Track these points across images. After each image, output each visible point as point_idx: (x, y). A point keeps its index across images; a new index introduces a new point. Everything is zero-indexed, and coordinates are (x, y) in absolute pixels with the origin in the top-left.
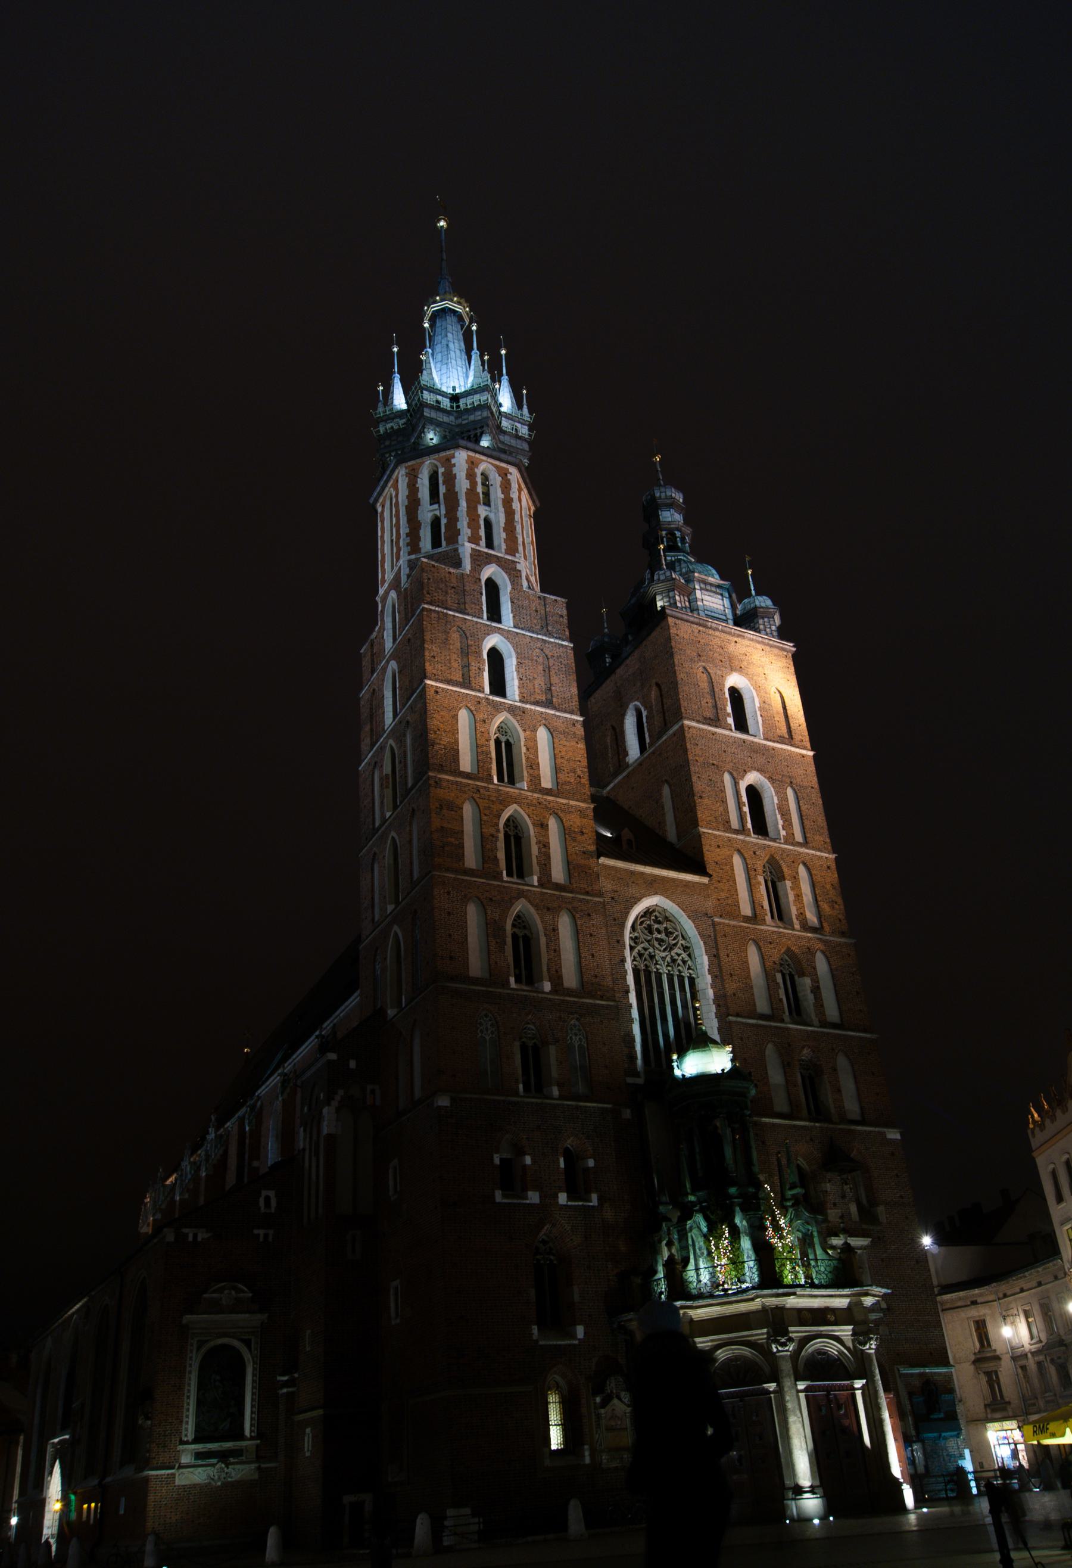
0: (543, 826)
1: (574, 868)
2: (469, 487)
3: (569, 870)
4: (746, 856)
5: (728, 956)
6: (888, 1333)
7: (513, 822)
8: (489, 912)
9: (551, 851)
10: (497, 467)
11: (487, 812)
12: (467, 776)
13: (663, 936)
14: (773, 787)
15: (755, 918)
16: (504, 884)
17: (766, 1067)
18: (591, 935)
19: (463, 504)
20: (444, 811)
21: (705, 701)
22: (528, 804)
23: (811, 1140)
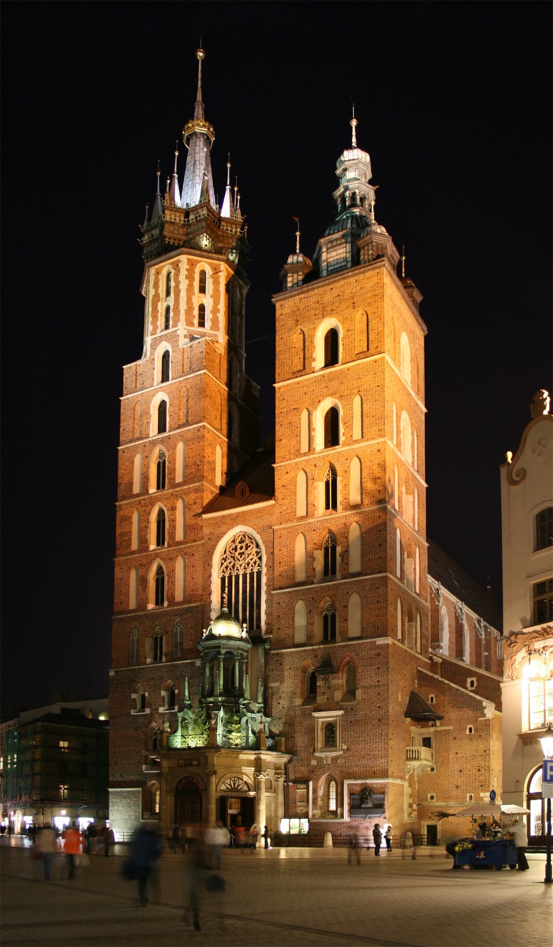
0: (173, 509)
2: (154, 294)
5: (280, 550)
6: (344, 763)
7: (163, 511)
10: (172, 264)
16: (149, 553)
17: (293, 617)
20: (123, 523)
23: (316, 657)
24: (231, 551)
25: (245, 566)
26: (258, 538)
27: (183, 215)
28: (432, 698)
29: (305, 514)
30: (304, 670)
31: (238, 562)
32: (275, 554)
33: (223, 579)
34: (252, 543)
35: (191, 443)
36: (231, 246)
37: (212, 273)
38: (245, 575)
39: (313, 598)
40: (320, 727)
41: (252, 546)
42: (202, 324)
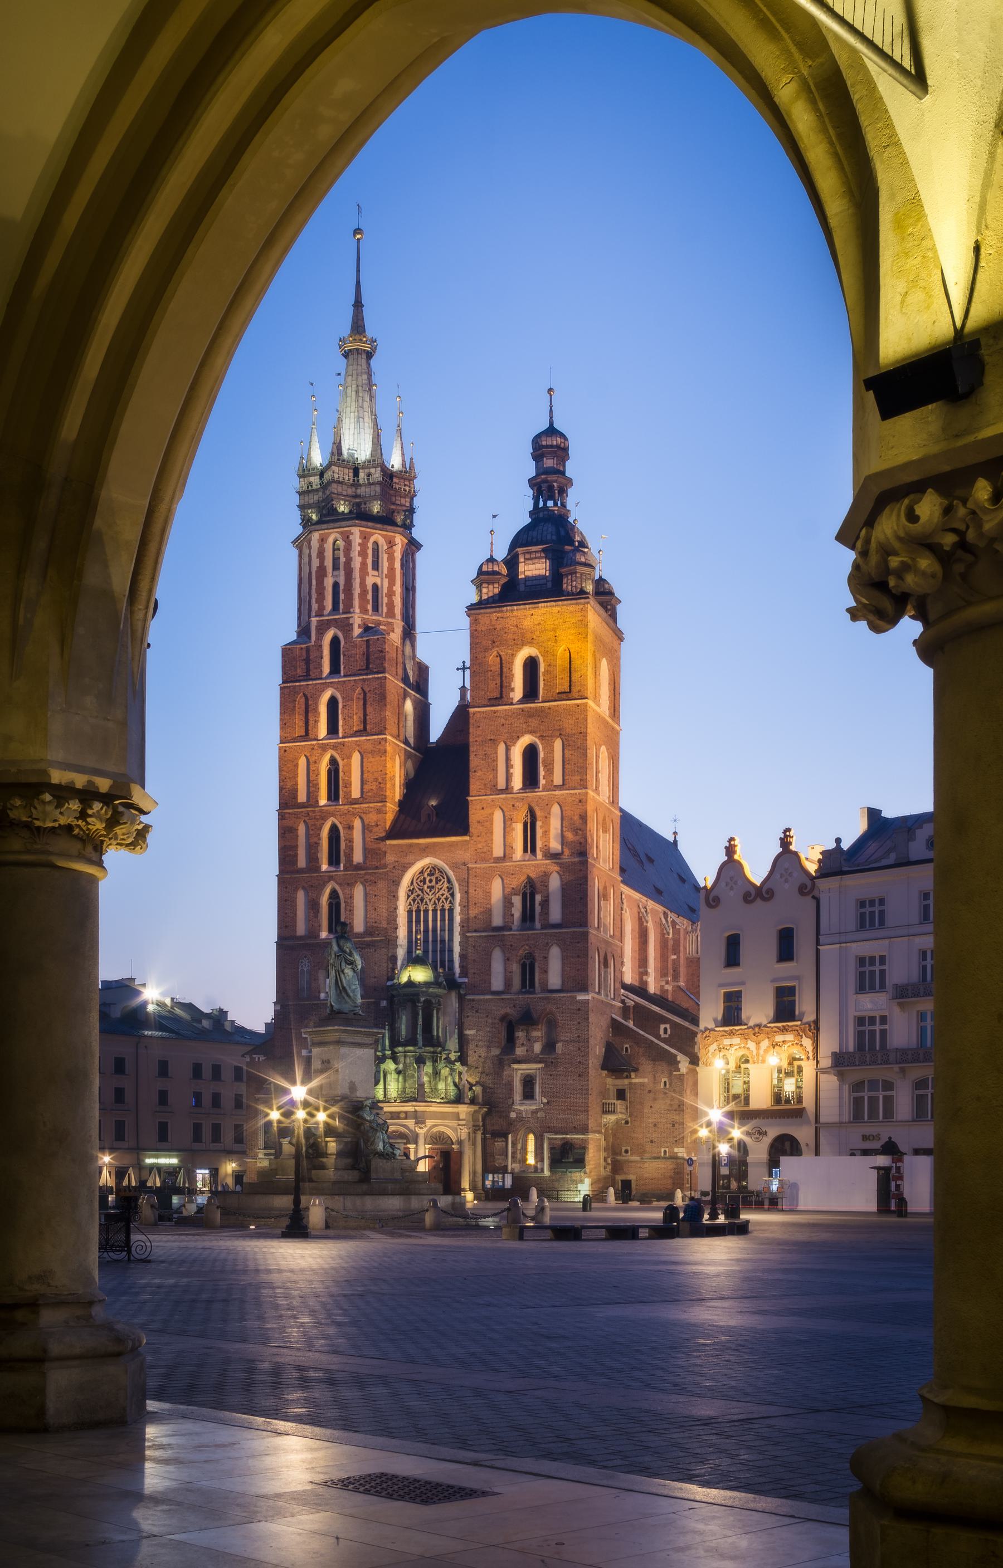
0: (350, 828)
1: (369, 853)
3: (366, 854)
4: (505, 810)
5: (475, 890)
8: (310, 894)
9: (354, 844)
11: (313, 828)
12: (303, 806)
13: (434, 883)
14: (542, 744)
15: (504, 858)
16: (321, 874)
18: (375, 896)
19: (314, 582)
21: (494, 682)
22: (341, 815)
24: (419, 883)
25: (435, 902)
26: (451, 873)
27: (351, 471)
28: (627, 1048)
29: (502, 855)
30: (503, 1018)
31: (427, 896)
32: (470, 894)
33: (410, 912)
34: (443, 877)
35: (370, 755)
36: (405, 508)
37: (385, 547)
38: (435, 911)
39: (511, 946)
40: (518, 1079)
41: (443, 880)
42: (376, 608)
